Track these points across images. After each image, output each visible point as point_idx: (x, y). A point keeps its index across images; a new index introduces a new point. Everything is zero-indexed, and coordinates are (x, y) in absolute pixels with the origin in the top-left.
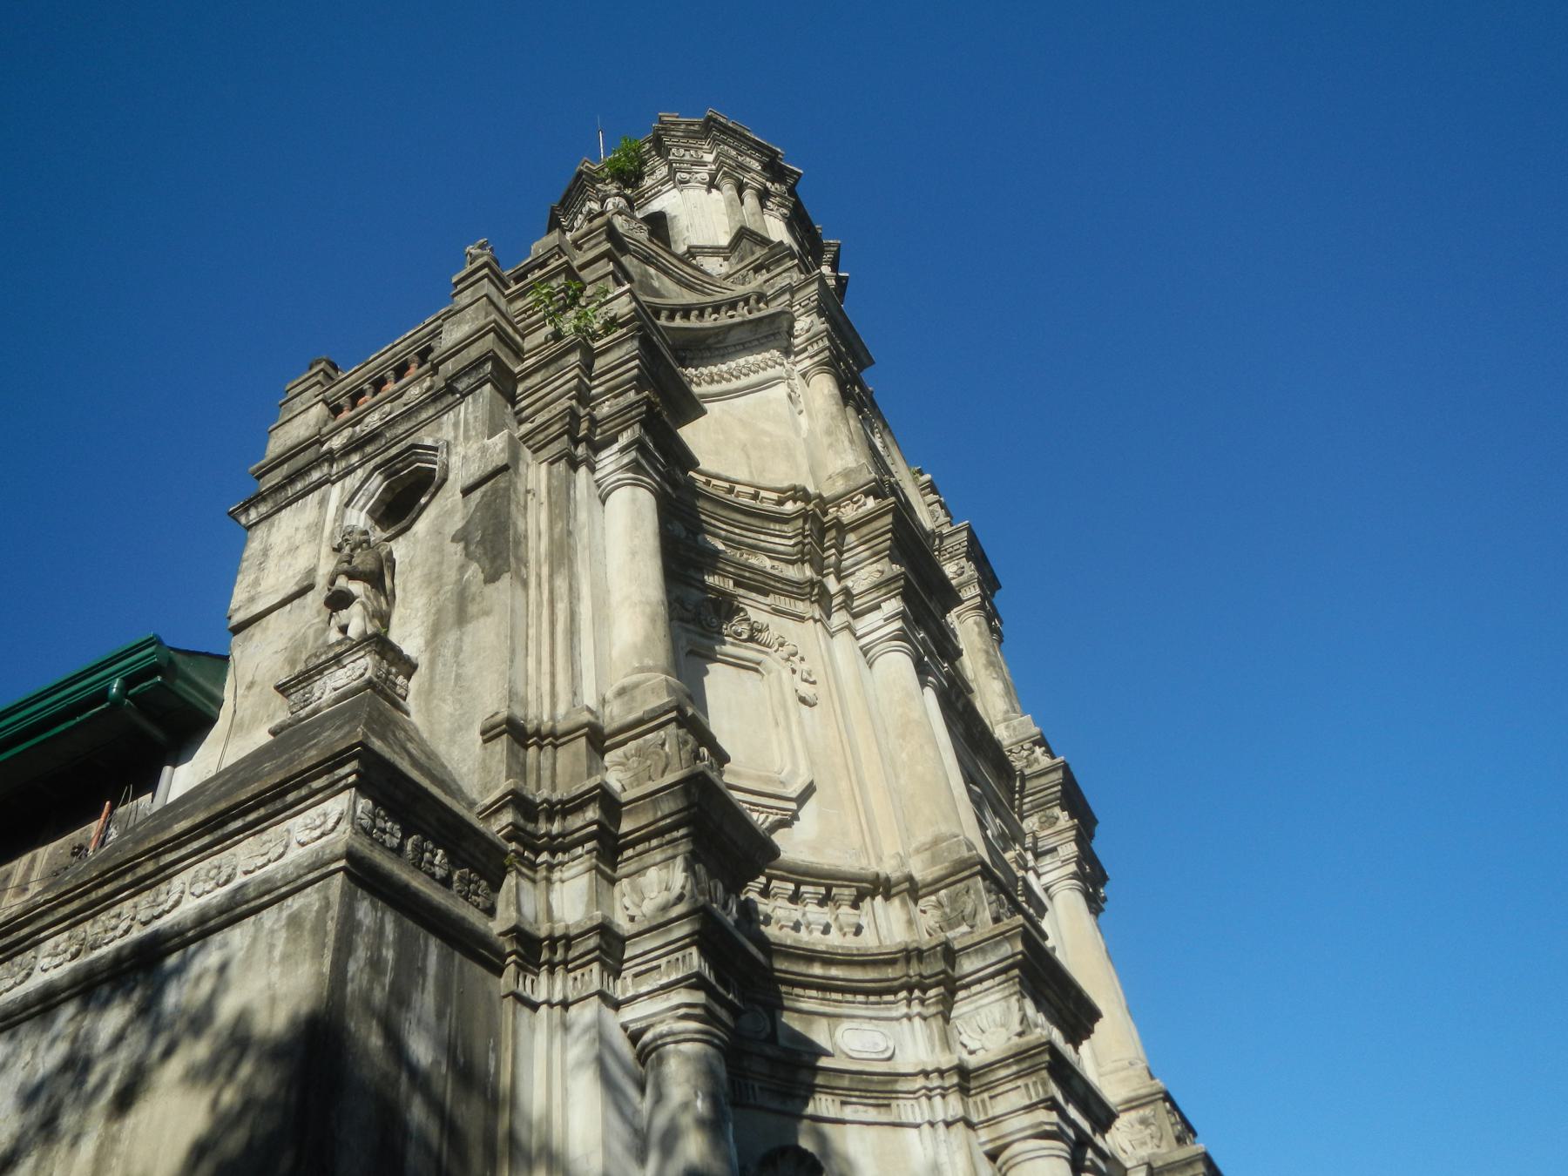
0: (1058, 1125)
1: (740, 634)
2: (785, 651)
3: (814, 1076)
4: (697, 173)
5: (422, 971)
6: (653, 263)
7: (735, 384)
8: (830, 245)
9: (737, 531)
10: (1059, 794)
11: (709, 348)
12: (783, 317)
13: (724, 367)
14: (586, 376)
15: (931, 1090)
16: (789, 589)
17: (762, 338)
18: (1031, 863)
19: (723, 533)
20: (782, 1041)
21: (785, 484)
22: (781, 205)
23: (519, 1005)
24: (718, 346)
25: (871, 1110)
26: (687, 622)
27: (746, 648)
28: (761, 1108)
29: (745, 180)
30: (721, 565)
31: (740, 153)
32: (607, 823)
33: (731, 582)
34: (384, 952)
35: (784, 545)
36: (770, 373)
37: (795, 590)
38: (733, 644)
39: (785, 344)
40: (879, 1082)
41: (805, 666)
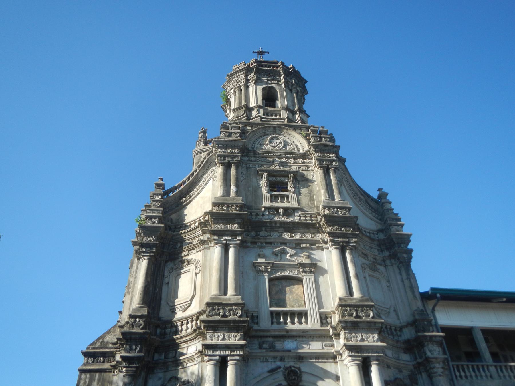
0: (208, 359)
1: (186, 265)
2: (195, 264)
3: (180, 361)
4: (231, 93)
5: (95, 380)
6: (203, 152)
7: (203, 185)
8: (280, 69)
9: (191, 236)
10: (326, 224)
11: (195, 183)
12: (210, 158)
13: (199, 184)
14: (141, 237)
15: (199, 356)
16: (198, 245)
17: (207, 168)
18: (323, 247)
19: (189, 238)
20: (177, 356)
21: (203, 214)
22: (253, 80)
23: (114, 376)
24: (197, 180)
25: (192, 363)
26: (176, 269)
27: (188, 267)
28: (171, 370)
29: (240, 85)
30: (183, 250)
31: (238, 77)
32: (121, 342)
33: (187, 251)
34: (87, 380)
35: (200, 233)
36: (211, 175)
37: (199, 244)
38: (185, 268)
39: (215, 163)
40: (192, 358)
41: (199, 264)
